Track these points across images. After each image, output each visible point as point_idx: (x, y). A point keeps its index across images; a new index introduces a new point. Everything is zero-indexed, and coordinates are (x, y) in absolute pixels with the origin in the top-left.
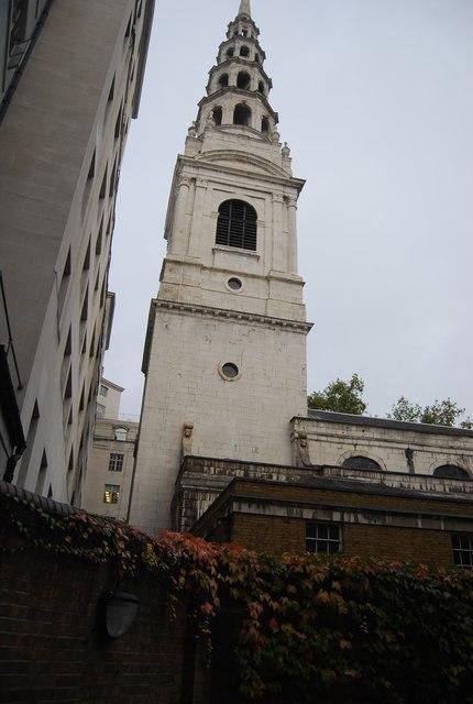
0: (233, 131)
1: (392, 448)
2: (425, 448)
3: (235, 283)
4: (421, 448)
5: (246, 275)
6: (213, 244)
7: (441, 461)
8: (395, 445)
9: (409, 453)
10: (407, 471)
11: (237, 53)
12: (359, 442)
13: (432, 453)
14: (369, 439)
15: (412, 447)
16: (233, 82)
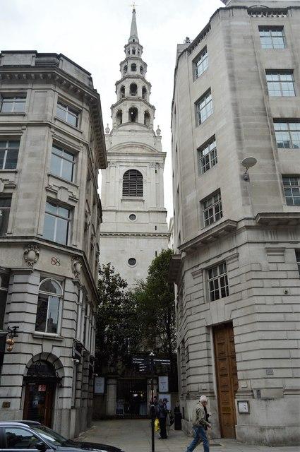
0: (129, 127)
3: (133, 217)
5: (138, 212)
6: (121, 197)
11: (129, 68)
16: (127, 90)
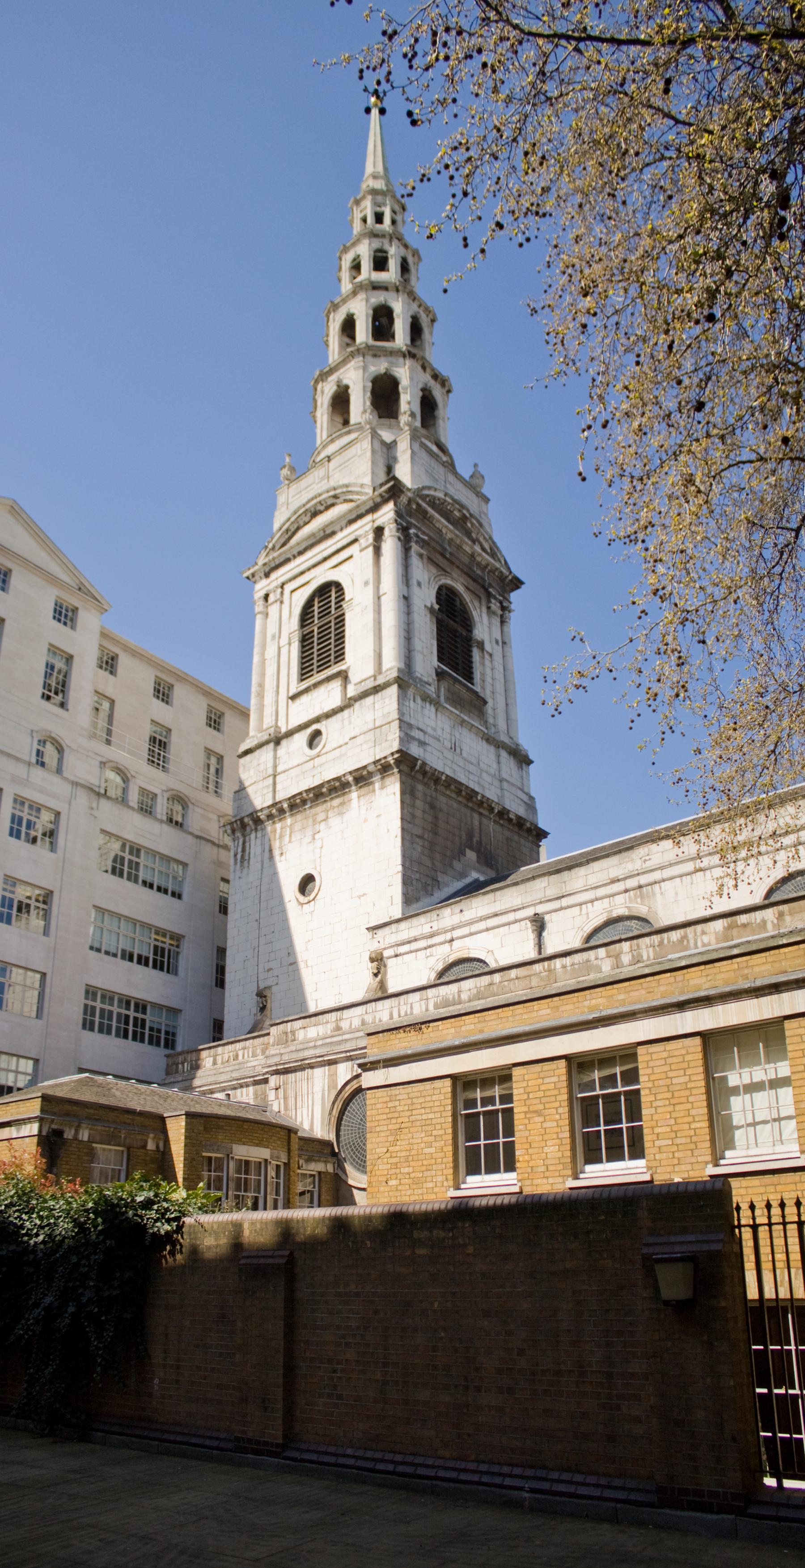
1: (509, 924)
2: (565, 902)
4: (556, 905)
7: (597, 915)
8: (511, 917)
9: (539, 924)
10: (532, 954)
12: (456, 933)
13: (581, 904)
14: (470, 923)
15: (540, 909)
